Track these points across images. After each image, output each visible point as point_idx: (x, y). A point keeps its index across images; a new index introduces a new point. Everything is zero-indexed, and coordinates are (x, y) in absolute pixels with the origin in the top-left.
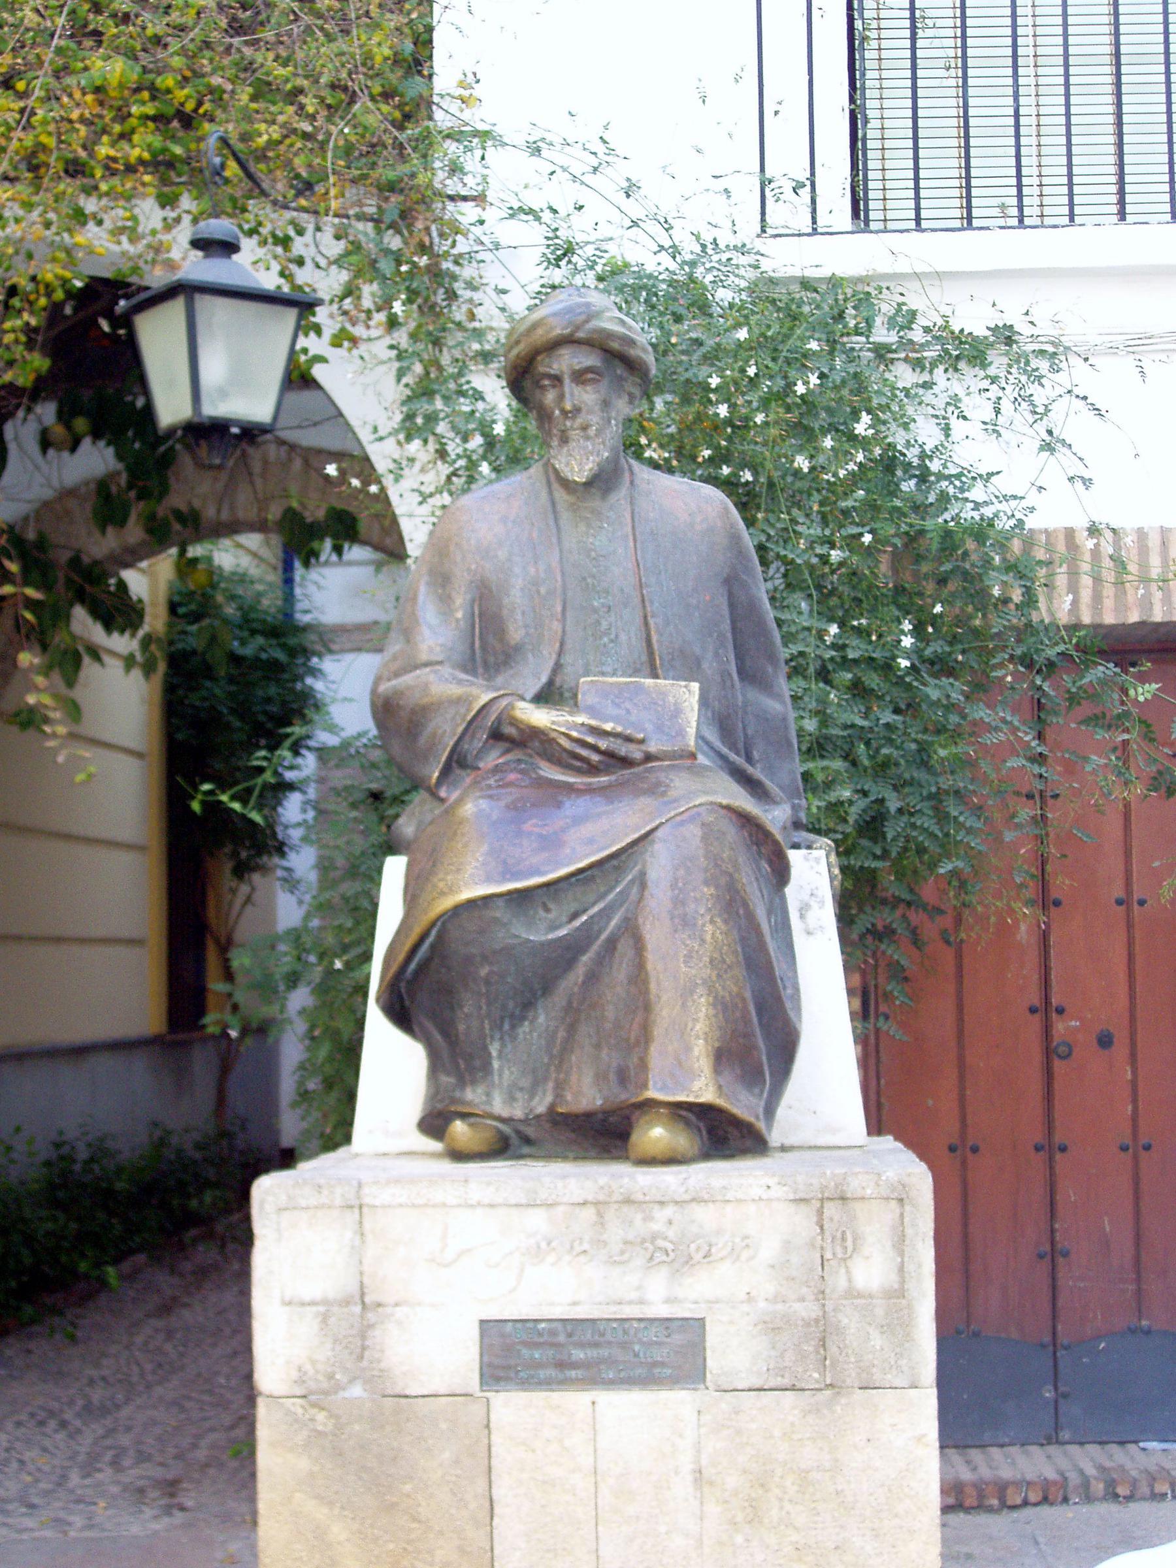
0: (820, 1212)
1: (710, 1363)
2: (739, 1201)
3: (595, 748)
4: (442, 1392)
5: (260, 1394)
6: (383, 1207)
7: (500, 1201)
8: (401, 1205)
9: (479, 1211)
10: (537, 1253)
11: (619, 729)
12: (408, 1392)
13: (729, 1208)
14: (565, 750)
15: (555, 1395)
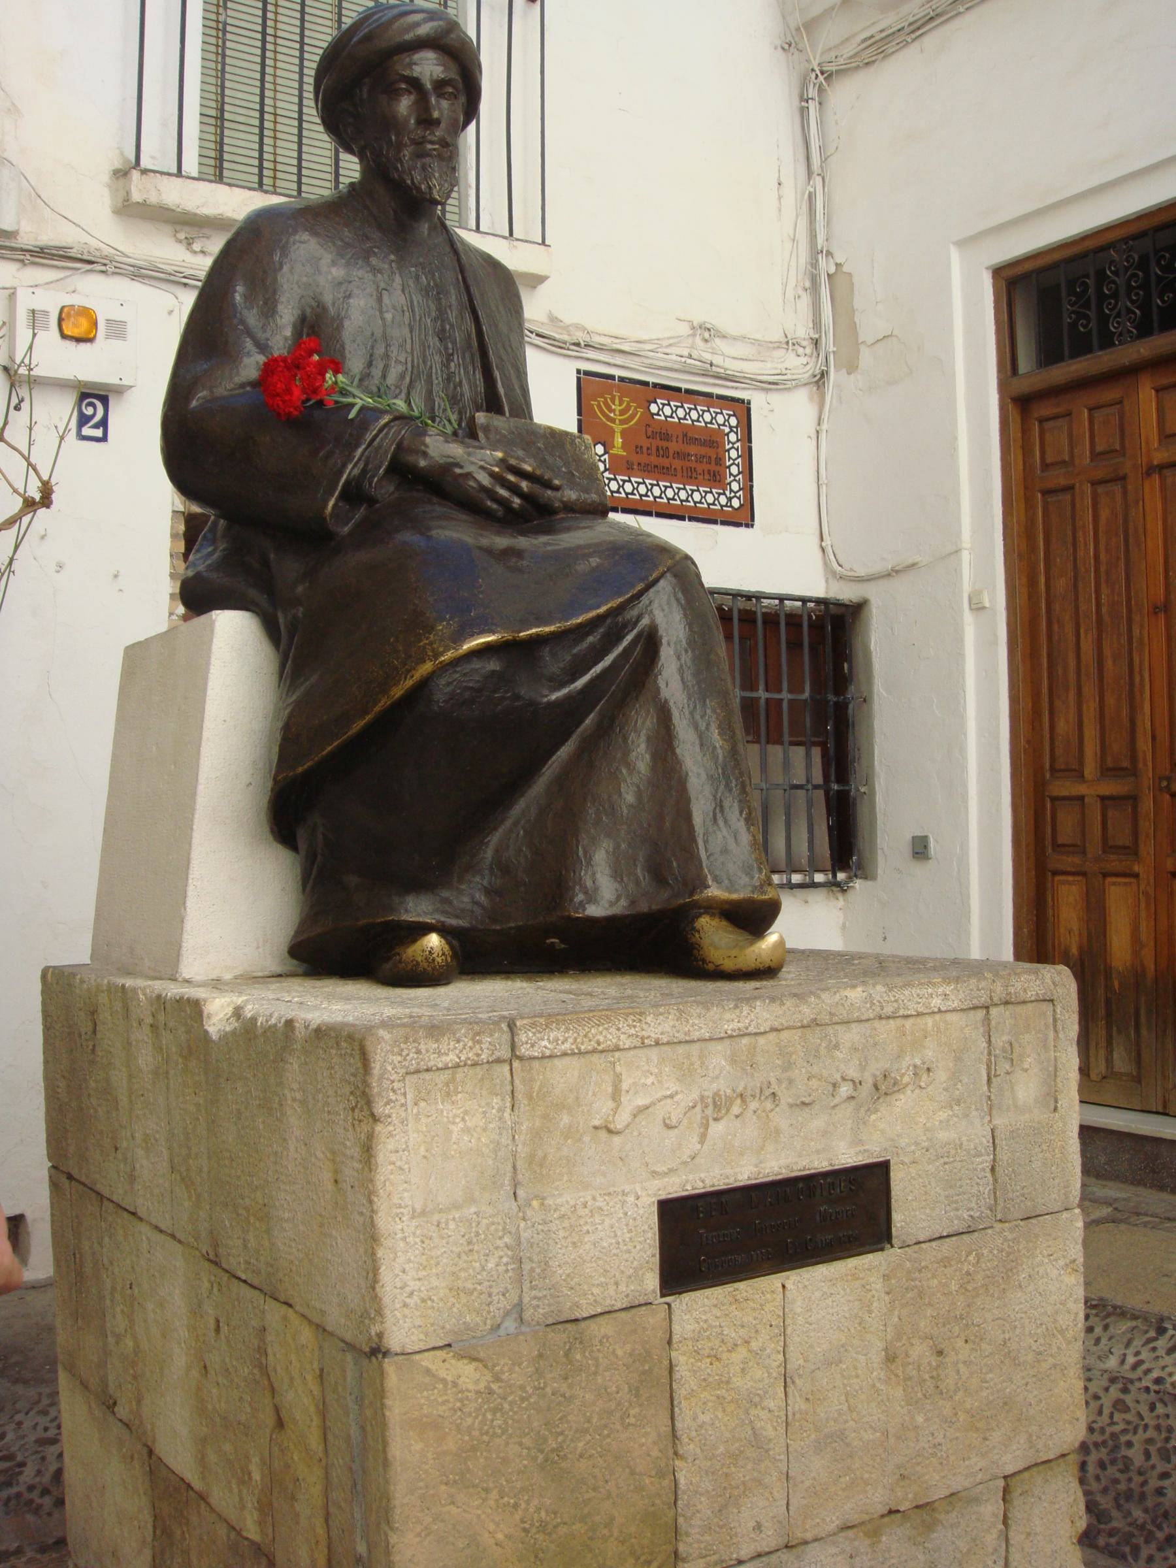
0: (987, 1020)
1: (897, 1217)
2: (919, 1014)
3: (514, 489)
4: (619, 1305)
5: (386, 1354)
6: (543, 1057)
7: (681, 1036)
8: (565, 1054)
9: (654, 1054)
10: (718, 1106)
11: (538, 472)
12: (578, 1315)
13: (908, 1023)
14: (483, 488)
15: (742, 1285)
